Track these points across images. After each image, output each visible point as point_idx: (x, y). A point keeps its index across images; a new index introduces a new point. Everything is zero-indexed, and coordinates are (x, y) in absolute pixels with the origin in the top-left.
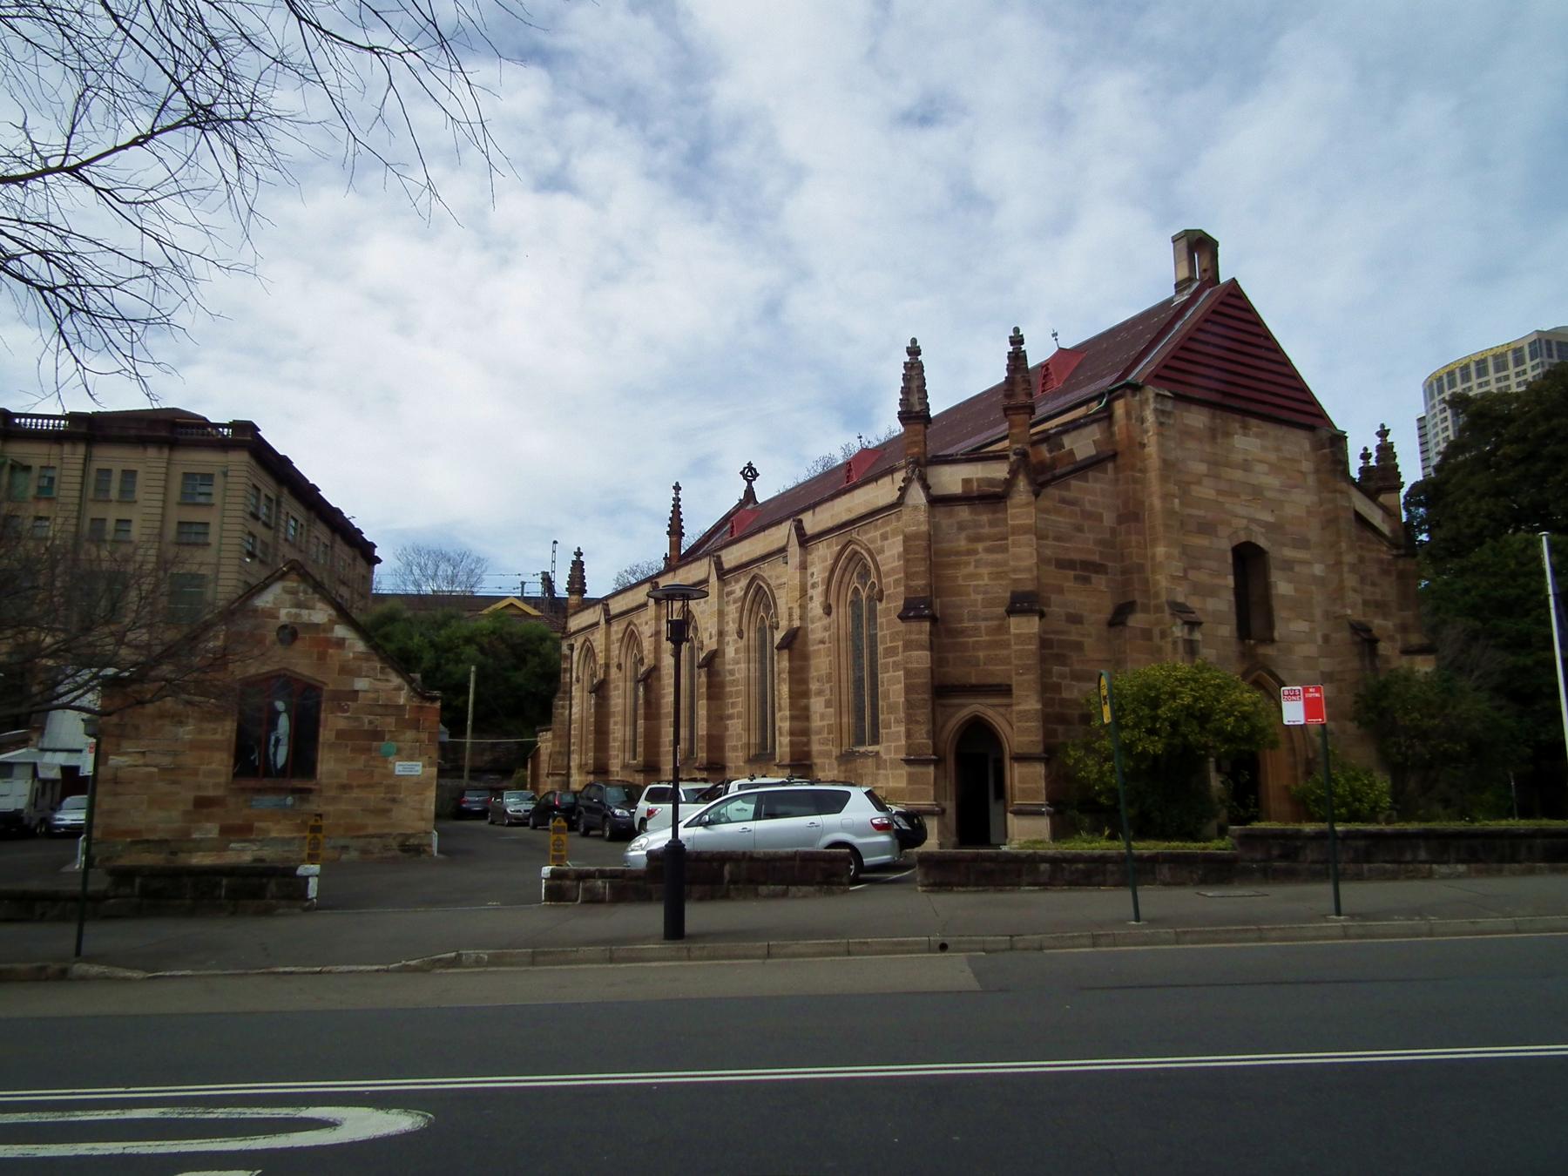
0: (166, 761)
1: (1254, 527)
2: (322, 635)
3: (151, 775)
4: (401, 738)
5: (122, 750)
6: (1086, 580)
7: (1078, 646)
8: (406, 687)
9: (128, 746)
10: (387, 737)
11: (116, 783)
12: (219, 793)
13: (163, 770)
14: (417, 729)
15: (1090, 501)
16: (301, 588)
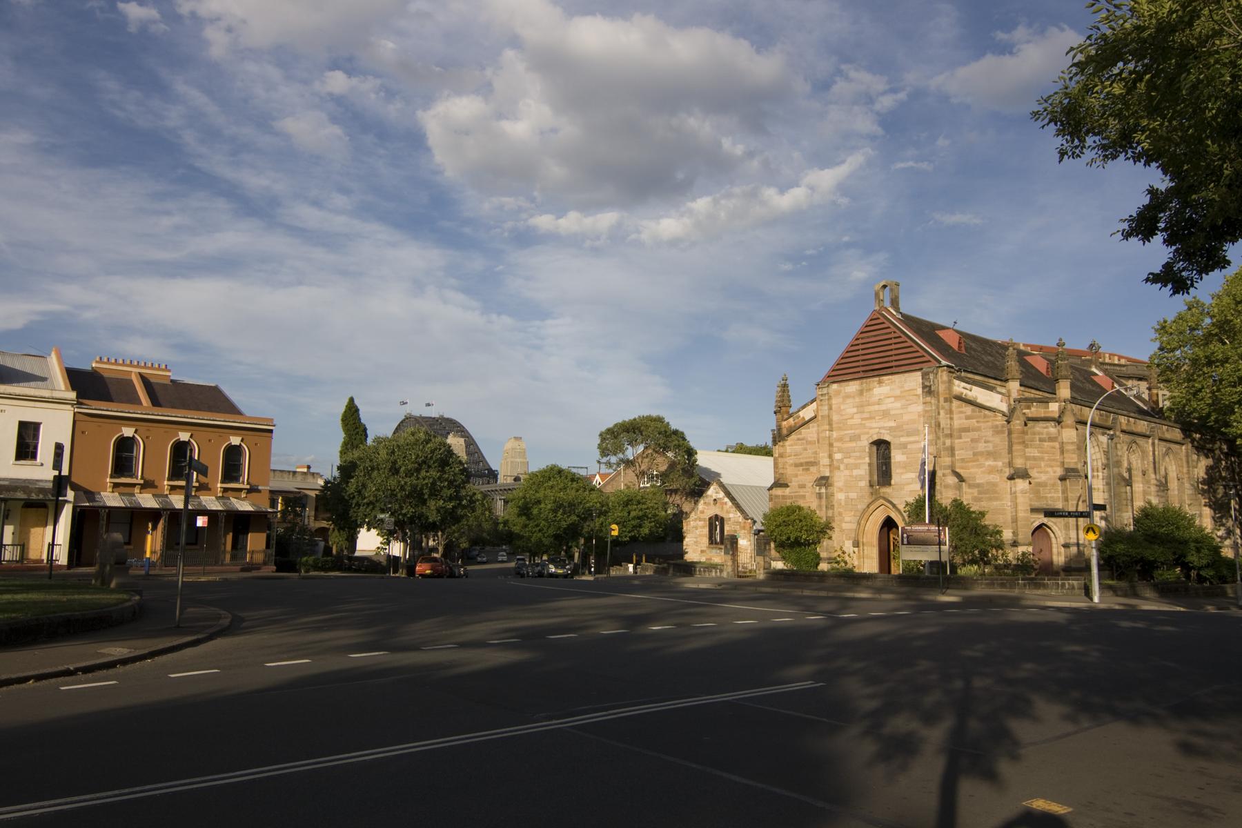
0: (695, 540)
1: (883, 431)
6: (808, 469)
7: (804, 497)
15: (810, 437)
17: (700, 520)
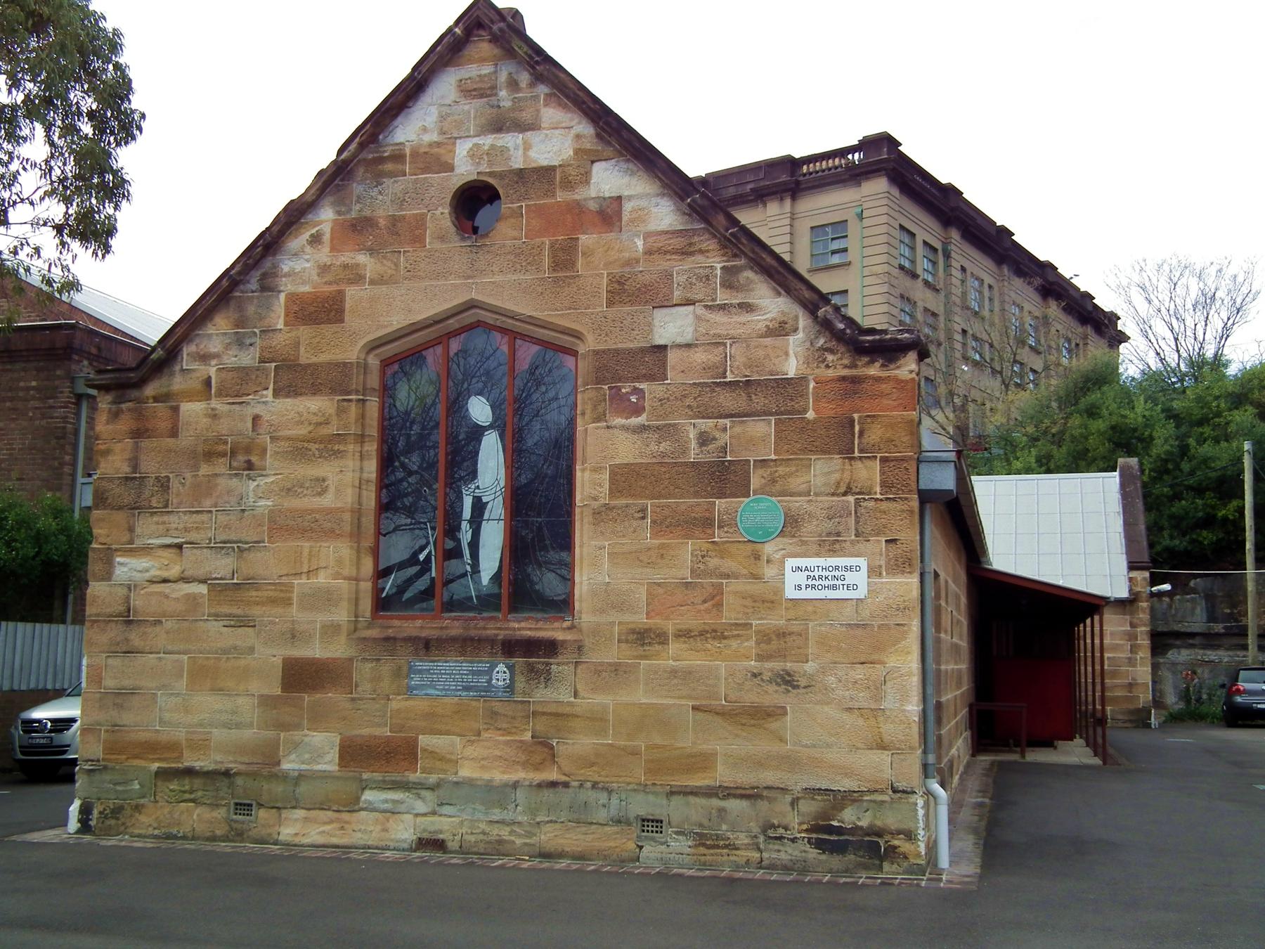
0: (221, 566)
2: (561, 196)
3: (193, 599)
4: (797, 483)
5: (138, 543)
8: (803, 321)
9: (149, 530)
10: (755, 481)
11: (129, 622)
12: (338, 650)
13: (223, 589)
14: (847, 452)
16: (503, 77)
17: (294, 377)
